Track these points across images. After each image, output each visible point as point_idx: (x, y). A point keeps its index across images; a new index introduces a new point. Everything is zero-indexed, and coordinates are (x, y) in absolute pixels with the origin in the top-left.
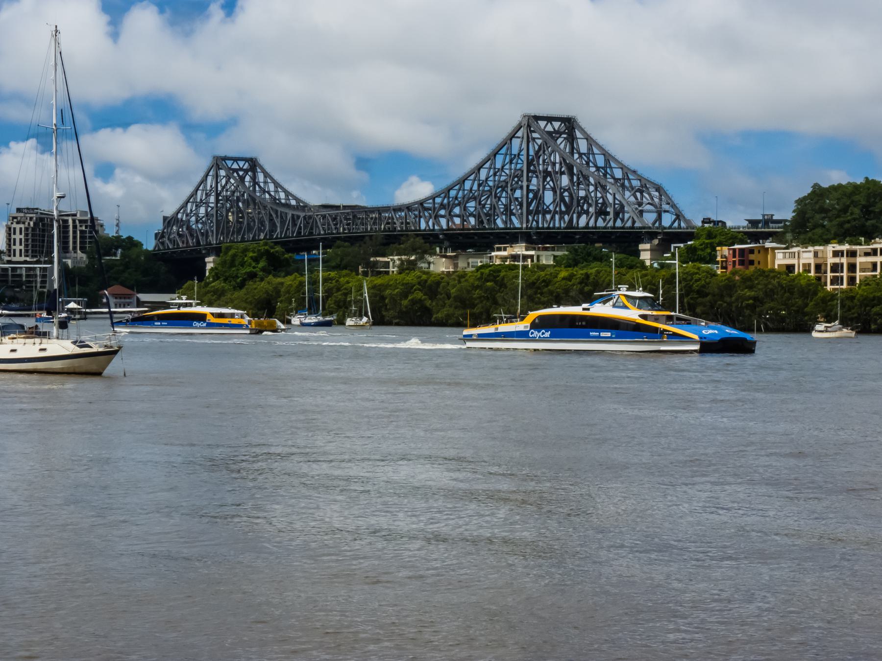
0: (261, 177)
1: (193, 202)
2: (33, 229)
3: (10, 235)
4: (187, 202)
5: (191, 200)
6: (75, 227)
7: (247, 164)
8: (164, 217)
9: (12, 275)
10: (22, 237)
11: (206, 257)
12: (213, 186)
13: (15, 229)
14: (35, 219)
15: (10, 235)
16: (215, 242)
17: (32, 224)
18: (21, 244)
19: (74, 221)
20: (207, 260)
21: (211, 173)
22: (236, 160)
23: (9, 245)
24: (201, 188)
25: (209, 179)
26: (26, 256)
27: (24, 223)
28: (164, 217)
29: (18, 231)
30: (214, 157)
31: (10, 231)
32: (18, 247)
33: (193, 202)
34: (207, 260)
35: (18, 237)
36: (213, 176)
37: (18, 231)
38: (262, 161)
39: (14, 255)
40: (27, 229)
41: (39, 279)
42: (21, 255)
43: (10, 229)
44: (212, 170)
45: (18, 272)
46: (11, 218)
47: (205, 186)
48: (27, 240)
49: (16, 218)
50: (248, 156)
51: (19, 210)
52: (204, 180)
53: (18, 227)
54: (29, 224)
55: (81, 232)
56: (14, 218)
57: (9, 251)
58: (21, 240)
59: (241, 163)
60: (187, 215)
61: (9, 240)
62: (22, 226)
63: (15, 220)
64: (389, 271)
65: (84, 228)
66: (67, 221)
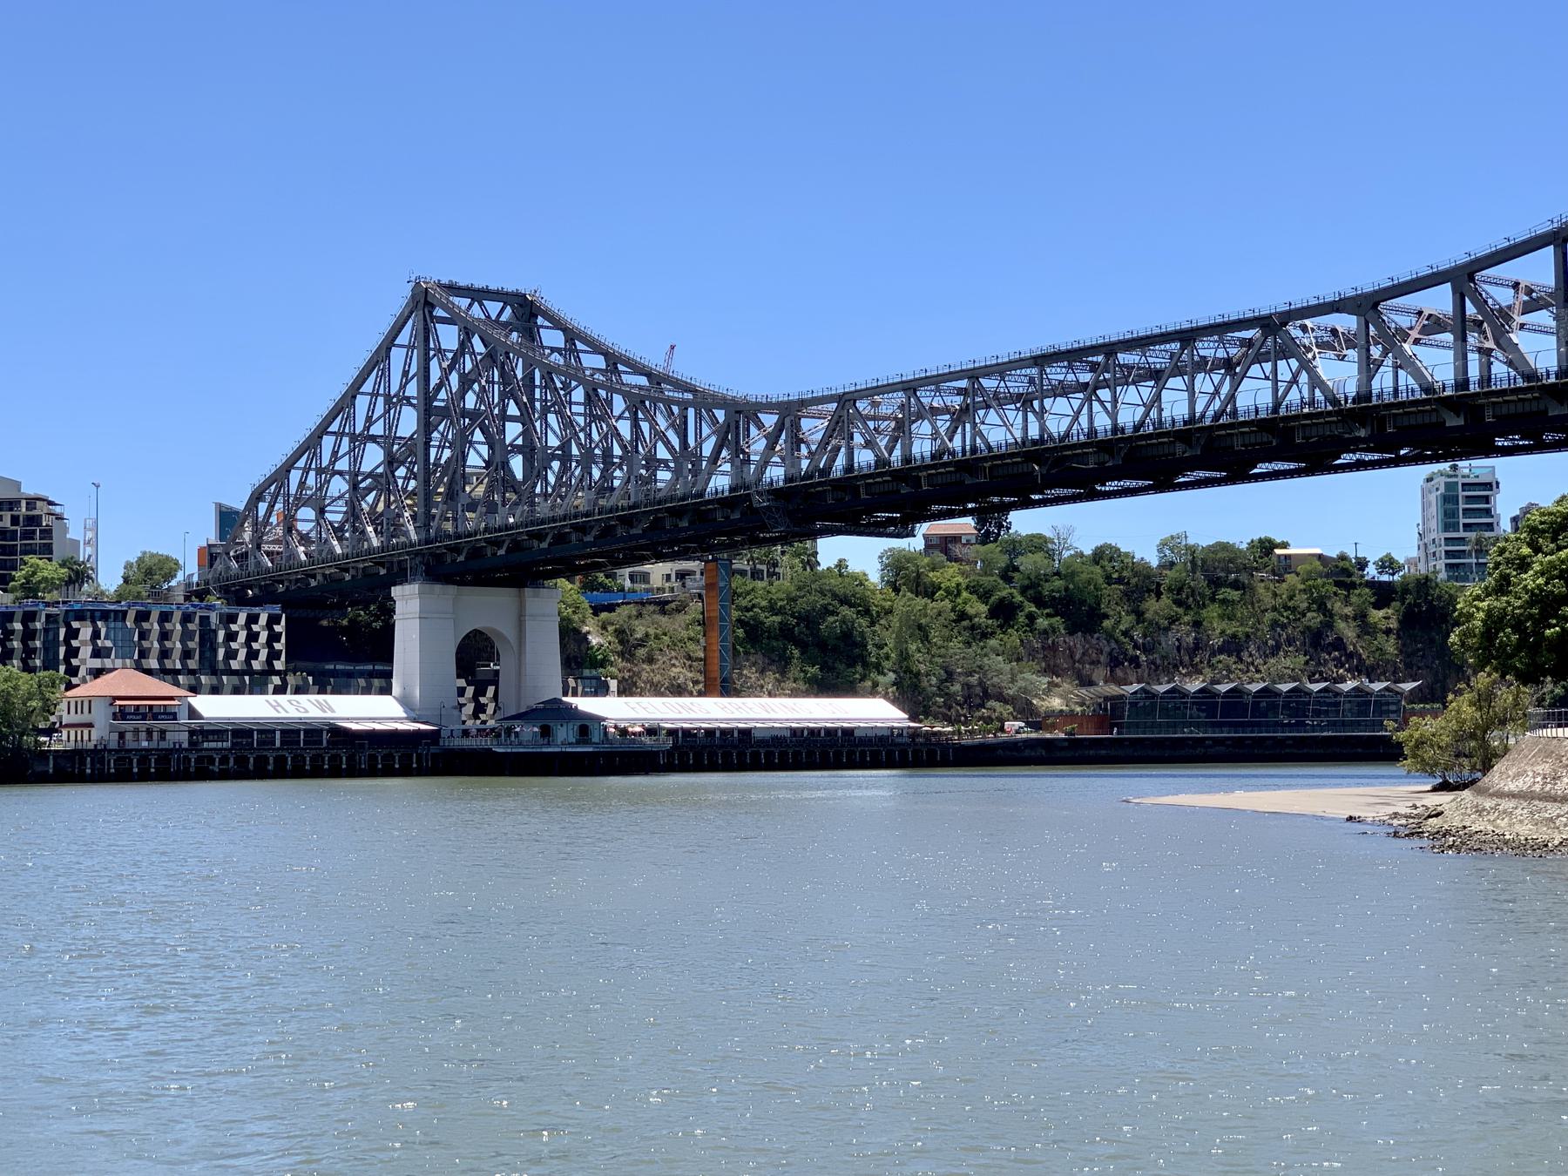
4: (322, 430)
5: (334, 427)
7: (508, 310)
8: (219, 506)
11: (395, 585)
12: (413, 370)
20: (396, 591)
21: (404, 337)
22: (479, 295)
24: (368, 387)
25: (397, 356)
28: (219, 506)
33: (339, 435)
34: (396, 591)
36: (411, 347)
38: (552, 299)
44: (410, 322)
47: (385, 374)
52: (380, 358)
59: (493, 307)
64: (1446, 545)
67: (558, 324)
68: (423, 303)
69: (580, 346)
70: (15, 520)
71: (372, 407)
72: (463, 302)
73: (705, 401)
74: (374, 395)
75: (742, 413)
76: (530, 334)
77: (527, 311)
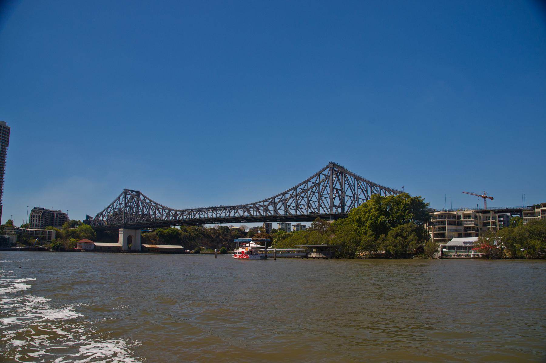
0: (142, 198)
1: (112, 208)
2: (42, 216)
3: (32, 218)
6: (57, 216)
9: (48, 234)
10: (37, 219)
13: (34, 215)
14: (42, 212)
15: (32, 218)
16: (123, 223)
17: (41, 213)
18: (36, 222)
19: (57, 214)
20: (120, 230)
21: (122, 196)
22: (132, 191)
23: (31, 222)
24: (116, 202)
26: (39, 226)
27: (38, 213)
29: (35, 217)
30: (125, 190)
31: (32, 217)
32: (35, 223)
34: (120, 230)
35: (35, 219)
37: (35, 217)
39: (33, 226)
40: (40, 216)
41: (47, 236)
42: (36, 226)
43: (32, 215)
45: (38, 233)
46: (32, 211)
48: (39, 220)
49: (35, 211)
50: (137, 190)
51: (35, 208)
52: (119, 198)
53: (35, 215)
54: (40, 213)
55: (59, 218)
56: (33, 211)
57: (31, 224)
58: (37, 220)
59: (134, 193)
60: (108, 213)
61: (31, 220)
62: (37, 214)
63: (34, 212)
65: (60, 217)
66: (53, 214)
67: (143, 196)
68: (126, 192)
69: (146, 199)
70: (61, 217)
71: (117, 204)
72: (130, 192)
73: (163, 208)
74: (117, 203)
75: (170, 210)
76: (139, 196)
77: (138, 193)
